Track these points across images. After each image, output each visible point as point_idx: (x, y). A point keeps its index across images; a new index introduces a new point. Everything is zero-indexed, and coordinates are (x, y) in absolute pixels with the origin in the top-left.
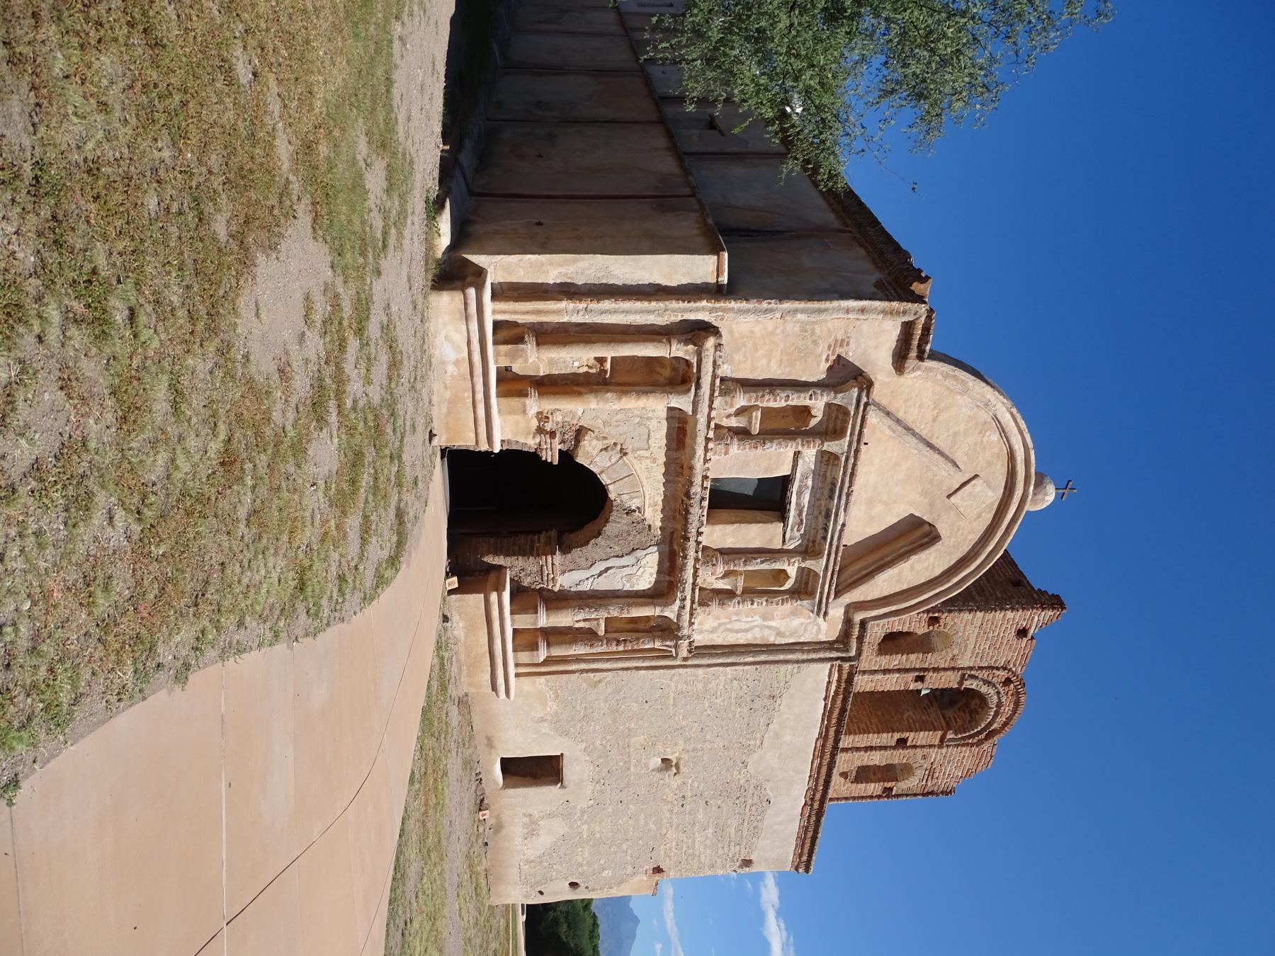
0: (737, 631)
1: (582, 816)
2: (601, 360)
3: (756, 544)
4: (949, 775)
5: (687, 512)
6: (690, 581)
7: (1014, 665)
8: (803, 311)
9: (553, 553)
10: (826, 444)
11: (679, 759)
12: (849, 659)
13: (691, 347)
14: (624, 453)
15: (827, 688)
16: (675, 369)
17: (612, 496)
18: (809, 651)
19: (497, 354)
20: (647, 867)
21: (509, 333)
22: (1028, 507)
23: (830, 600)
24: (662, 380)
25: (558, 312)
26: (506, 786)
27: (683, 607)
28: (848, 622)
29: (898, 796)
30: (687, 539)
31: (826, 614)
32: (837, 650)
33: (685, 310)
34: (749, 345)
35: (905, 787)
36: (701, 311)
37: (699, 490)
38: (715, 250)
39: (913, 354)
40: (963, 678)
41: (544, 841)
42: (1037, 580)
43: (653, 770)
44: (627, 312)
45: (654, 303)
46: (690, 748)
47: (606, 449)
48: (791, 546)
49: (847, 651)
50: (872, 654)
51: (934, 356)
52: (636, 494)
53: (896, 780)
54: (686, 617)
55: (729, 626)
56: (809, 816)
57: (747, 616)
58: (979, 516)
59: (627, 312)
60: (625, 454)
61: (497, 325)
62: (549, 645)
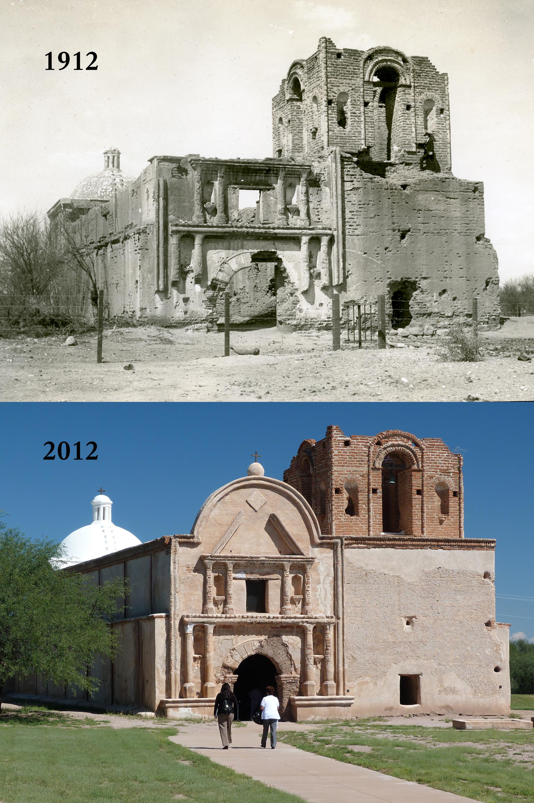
0: (326, 595)
1: (442, 665)
2: (195, 659)
3: (279, 591)
4: (445, 461)
5: (259, 623)
6: (293, 620)
7: (368, 442)
8: (175, 585)
9: (280, 678)
10: (229, 569)
11: (406, 617)
12: (342, 541)
13: (188, 626)
14: (234, 649)
15: (361, 548)
16: (199, 631)
17: (253, 653)
18: (337, 561)
19: (190, 697)
20: (485, 630)
21: (183, 693)
22: (262, 476)
23: (305, 557)
24: (203, 635)
25: (175, 675)
26: (420, 703)
27: (307, 622)
28: (321, 545)
29: (460, 488)
30: (272, 623)
31: (312, 558)
32: (337, 548)
33: (175, 629)
34: (189, 603)
35: (453, 485)
36: (175, 623)
37: (248, 619)
38: (153, 618)
39: (192, 540)
40: (375, 469)
41: (460, 685)
42: (323, 436)
43: (413, 630)
44: (176, 650)
45: (172, 641)
46: (398, 612)
47: (232, 656)
48: (280, 577)
49: (337, 543)
50: (358, 519)
51: (192, 532)
52: (253, 644)
53: (448, 490)
54: (312, 620)
55: (323, 599)
56: (450, 545)
57: (317, 591)
58: (267, 495)
59: (176, 650)
60: (234, 649)
61: (181, 697)
62: (327, 680)
